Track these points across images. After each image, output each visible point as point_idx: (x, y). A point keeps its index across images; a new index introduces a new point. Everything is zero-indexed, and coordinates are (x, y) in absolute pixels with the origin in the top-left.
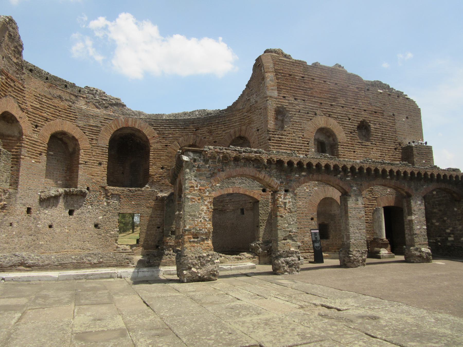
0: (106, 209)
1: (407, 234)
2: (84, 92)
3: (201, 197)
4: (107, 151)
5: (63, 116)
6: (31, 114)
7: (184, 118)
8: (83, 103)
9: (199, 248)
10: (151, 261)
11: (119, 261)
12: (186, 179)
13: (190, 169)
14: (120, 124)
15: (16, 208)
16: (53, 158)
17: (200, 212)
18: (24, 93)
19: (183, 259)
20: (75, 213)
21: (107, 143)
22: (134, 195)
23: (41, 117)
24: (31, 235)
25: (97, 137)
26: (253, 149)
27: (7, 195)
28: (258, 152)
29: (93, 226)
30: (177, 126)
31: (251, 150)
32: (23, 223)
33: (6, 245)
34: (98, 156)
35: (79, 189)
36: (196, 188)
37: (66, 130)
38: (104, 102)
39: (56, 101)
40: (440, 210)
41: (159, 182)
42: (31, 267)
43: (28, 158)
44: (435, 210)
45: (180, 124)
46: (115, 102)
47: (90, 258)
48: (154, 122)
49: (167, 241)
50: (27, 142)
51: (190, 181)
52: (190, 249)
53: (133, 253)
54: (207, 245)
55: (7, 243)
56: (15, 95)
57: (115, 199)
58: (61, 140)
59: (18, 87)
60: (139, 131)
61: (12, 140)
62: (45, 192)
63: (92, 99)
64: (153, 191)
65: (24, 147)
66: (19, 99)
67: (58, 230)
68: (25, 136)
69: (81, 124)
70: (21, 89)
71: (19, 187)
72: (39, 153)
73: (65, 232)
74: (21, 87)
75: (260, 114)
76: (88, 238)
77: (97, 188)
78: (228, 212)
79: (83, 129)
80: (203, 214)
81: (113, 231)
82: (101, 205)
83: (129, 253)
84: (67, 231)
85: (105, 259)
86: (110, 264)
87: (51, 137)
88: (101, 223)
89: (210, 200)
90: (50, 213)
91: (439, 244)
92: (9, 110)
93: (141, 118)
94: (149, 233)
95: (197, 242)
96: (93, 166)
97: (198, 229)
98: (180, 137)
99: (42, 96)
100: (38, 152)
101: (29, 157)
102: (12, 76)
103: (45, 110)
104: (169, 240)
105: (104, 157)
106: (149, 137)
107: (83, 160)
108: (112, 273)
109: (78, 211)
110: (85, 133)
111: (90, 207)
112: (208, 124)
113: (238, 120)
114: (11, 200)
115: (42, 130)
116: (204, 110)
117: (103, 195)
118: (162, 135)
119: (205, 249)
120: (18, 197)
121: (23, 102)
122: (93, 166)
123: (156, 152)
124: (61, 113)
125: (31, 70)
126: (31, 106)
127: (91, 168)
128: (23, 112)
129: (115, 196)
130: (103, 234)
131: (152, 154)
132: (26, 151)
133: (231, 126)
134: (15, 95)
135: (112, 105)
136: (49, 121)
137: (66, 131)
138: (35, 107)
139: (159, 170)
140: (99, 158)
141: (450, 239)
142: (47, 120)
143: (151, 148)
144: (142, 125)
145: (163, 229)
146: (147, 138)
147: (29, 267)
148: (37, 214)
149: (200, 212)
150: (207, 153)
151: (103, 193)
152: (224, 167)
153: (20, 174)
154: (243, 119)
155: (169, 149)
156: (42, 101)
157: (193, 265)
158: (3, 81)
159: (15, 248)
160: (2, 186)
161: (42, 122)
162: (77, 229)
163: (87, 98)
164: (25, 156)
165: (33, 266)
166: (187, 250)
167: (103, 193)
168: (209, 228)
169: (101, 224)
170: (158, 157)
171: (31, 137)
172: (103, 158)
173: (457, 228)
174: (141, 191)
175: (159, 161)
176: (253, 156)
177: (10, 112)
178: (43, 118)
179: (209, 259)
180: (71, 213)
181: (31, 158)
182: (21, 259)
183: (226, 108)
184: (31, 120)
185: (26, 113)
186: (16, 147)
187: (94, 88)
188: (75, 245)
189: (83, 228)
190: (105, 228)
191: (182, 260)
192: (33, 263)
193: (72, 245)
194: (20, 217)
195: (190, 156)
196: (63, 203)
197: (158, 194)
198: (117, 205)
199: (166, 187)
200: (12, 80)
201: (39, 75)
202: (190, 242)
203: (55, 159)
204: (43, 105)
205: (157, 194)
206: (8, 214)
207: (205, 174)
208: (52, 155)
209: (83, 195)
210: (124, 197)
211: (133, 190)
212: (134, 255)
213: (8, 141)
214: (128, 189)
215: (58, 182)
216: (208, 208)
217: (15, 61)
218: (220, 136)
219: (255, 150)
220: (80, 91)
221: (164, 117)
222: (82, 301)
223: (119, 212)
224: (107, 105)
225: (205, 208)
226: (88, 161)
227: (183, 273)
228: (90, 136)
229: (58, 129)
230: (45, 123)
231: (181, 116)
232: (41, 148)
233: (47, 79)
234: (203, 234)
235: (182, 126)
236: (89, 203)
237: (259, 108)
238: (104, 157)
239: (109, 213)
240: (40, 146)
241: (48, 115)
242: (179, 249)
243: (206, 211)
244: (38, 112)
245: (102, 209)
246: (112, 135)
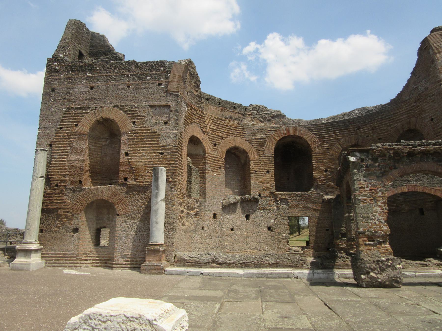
0: (276, 213)
2: (249, 110)
3: (373, 198)
4: (273, 160)
5: (234, 133)
6: (211, 135)
7: (344, 119)
8: (249, 120)
9: (376, 251)
10: (324, 264)
11: (294, 262)
12: (355, 180)
13: (358, 170)
14: (282, 134)
15: (205, 215)
16: (229, 170)
17: (374, 213)
18: (204, 119)
19: (360, 262)
20: (250, 218)
21: (272, 152)
22: (301, 199)
23: (218, 137)
24: (218, 237)
25: (263, 148)
26: (430, 141)
27: (198, 204)
28: (438, 144)
29: (267, 228)
30: (337, 128)
31: (428, 142)
32: (212, 227)
33: (200, 245)
34: (266, 165)
35: (252, 196)
36: (366, 189)
37: (237, 145)
38: (267, 116)
39: (228, 121)
41: (324, 185)
42: (221, 264)
43: (211, 172)
45: (340, 126)
46: (276, 114)
47: (268, 258)
48: (313, 127)
49: (338, 243)
50: (210, 158)
51: (359, 182)
52: (367, 253)
53: (304, 255)
54: (385, 248)
55: (201, 244)
56: (198, 122)
57: (284, 204)
58: (234, 154)
59: (200, 115)
60: (300, 138)
61: (198, 158)
62: (225, 199)
63: (256, 115)
64: (318, 194)
65: (208, 163)
66: (201, 124)
67: (238, 233)
68: (208, 154)
69: (249, 138)
70: (202, 116)
71: (207, 196)
72: (219, 167)
73: (244, 234)
74: (202, 114)
75: (433, 101)
76: (264, 239)
77: (267, 194)
78: (403, 212)
79: (251, 142)
80: (377, 216)
81: (284, 234)
82: (272, 210)
84: (245, 233)
85: (281, 260)
86: (286, 264)
87: (226, 153)
88: (273, 226)
89: (384, 201)
90: (231, 218)
92: (194, 134)
93: (301, 126)
94: (318, 235)
95: (373, 246)
96: (262, 175)
97: (373, 231)
98: (341, 139)
99: (217, 119)
100: (218, 166)
101: (211, 171)
102: (195, 106)
103: (220, 131)
104: (339, 242)
105: (270, 165)
106: (310, 143)
107: (253, 169)
108: (289, 273)
109: (253, 215)
110: (253, 145)
111: (262, 211)
112: (369, 122)
113: (405, 112)
114: (202, 208)
115: (219, 147)
116: (364, 108)
117: (273, 200)
118: (322, 139)
119: (383, 253)
120: (207, 205)
121: (204, 126)
122: (262, 175)
123: (318, 155)
124: (232, 131)
125: (207, 99)
126: (210, 128)
127: (261, 177)
128: (205, 134)
129: (284, 200)
130: (276, 237)
131: (315, 158)
132: (209, 166)
133: (397, 120)
134: (198, 122)
135: (273, 117)
136: (224, 139)
137: (238, 146)
138: (213, 129)
139: (323, 173)
140: (267, 167)
142: (222, 138)
143: (313, 153)
144: (302, 132)
145: (332, 232)
146: (308, 143)
147: (220, 264)
148: (221, 219)
149: (374, 213)
150: (375, 151)
151: (272, 199)
152: (397, 165)
153: (207, 186)
154: (412, 110)
155: (331, 152)
156: (217, 123)
157: (371, 269)
158: (189, 111)
159: (207, 248)
160: (195, 196)
161: (219, 141)
162: (253, 232)
163: (252, 115)
164: (209, 171)
165: (223, 264)
166: (363, 254)
167: (272, 199)
168: (386, 230)
169: (273, 227)
170: (320, 161)
171: (212, 154)
172: (270, 166)
174: (307, 194)
175: (321, 165)
176: (432, 149)
177: (196, 135)
178: (219, 137)
179: (389, 264)
180: (247, 217)
181: (213, 171)
182: (213, 257)
183: (389, 101)
184: (211, 140)
185: (207, 135)
186: (202, 164)
187: (257, 105)
188: (253, 246)
189: (258, 231)
190: (277, 231)
191: (359, 264)
192: (222, 261)
193: (250, 246)
194: (209, 222)
195: (356, 156)
196: (241, 209)
197: (324, 196)
198: (286, 209)
199: (331, 190)
200: (195, 110)
201: (213, 102)
202: (366, 245)
203: (231, 171)
204: (219, 126)
205: (323, 197)
206: (200, 220)
207: (375, 173)
208: (229, 168)
209: (256, 201)
210: (292, 201)
211: (299, 194)
212: (305, 256)
213: (196, 159)
214: (295, 194)
215: (235, 191)
216: (383, 209)
217: (196, 93)
218: (384, 133)
219: (433, 142)
220: (246, 110)
221: (323, 121)
222: (268, 298)
223: (288, 215)
224: (269, 118)
225: (379, 209)
226: (258, 170)
227: (361, 277)
228: (257, 148)
229: (232, 145)
230: (221, 141)
231: (340, 118)
232: (220, 162)
233: (220, 104)
234: (379, 237)
235: (342, 128)
236: (261, 208)
237: (430, 95)
238: (270, 165)
239: (279, 216)
240: (219, 161)
241: (223, 134)
242: (353, 252)
243: (380, 212)
244: (215, 133)
245: (273, 213)
246: (276, 145)
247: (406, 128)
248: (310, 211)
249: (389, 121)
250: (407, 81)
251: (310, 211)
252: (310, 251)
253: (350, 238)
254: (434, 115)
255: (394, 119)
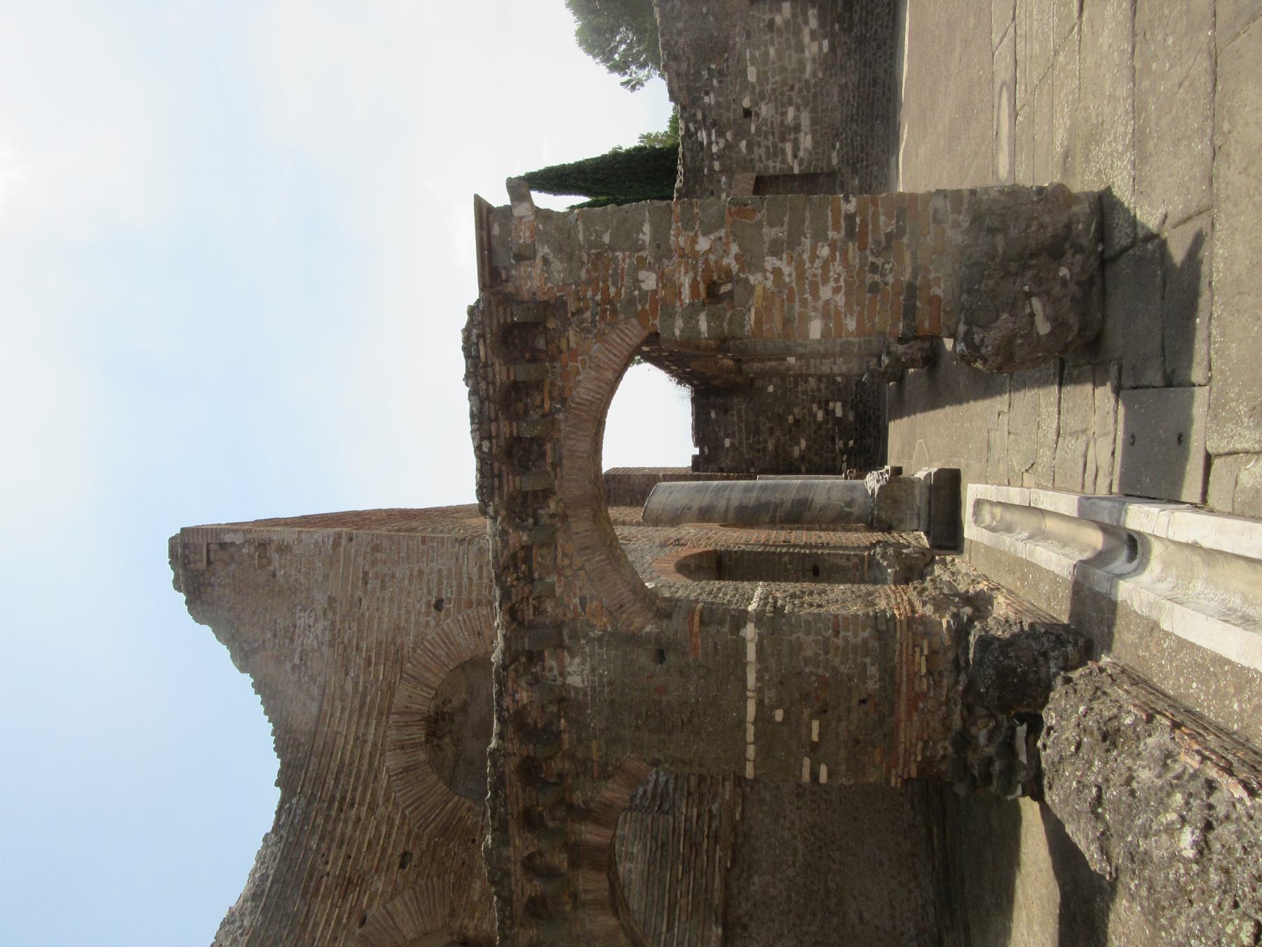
1: (831, 369)
40: (771, 431)
44: (770, 447)
91: (851, 443)
112: (304, 895)
113: (358, 724)
133: (370, 764)
141: (839, 413)
173: (812, 390)
183: (278, 792)
218: (388, 835)
247: (419, 734)
249: (352, 805)
250: (256, 693)
253: (875, 628)
254: (429, 593)
255: (357, 779)
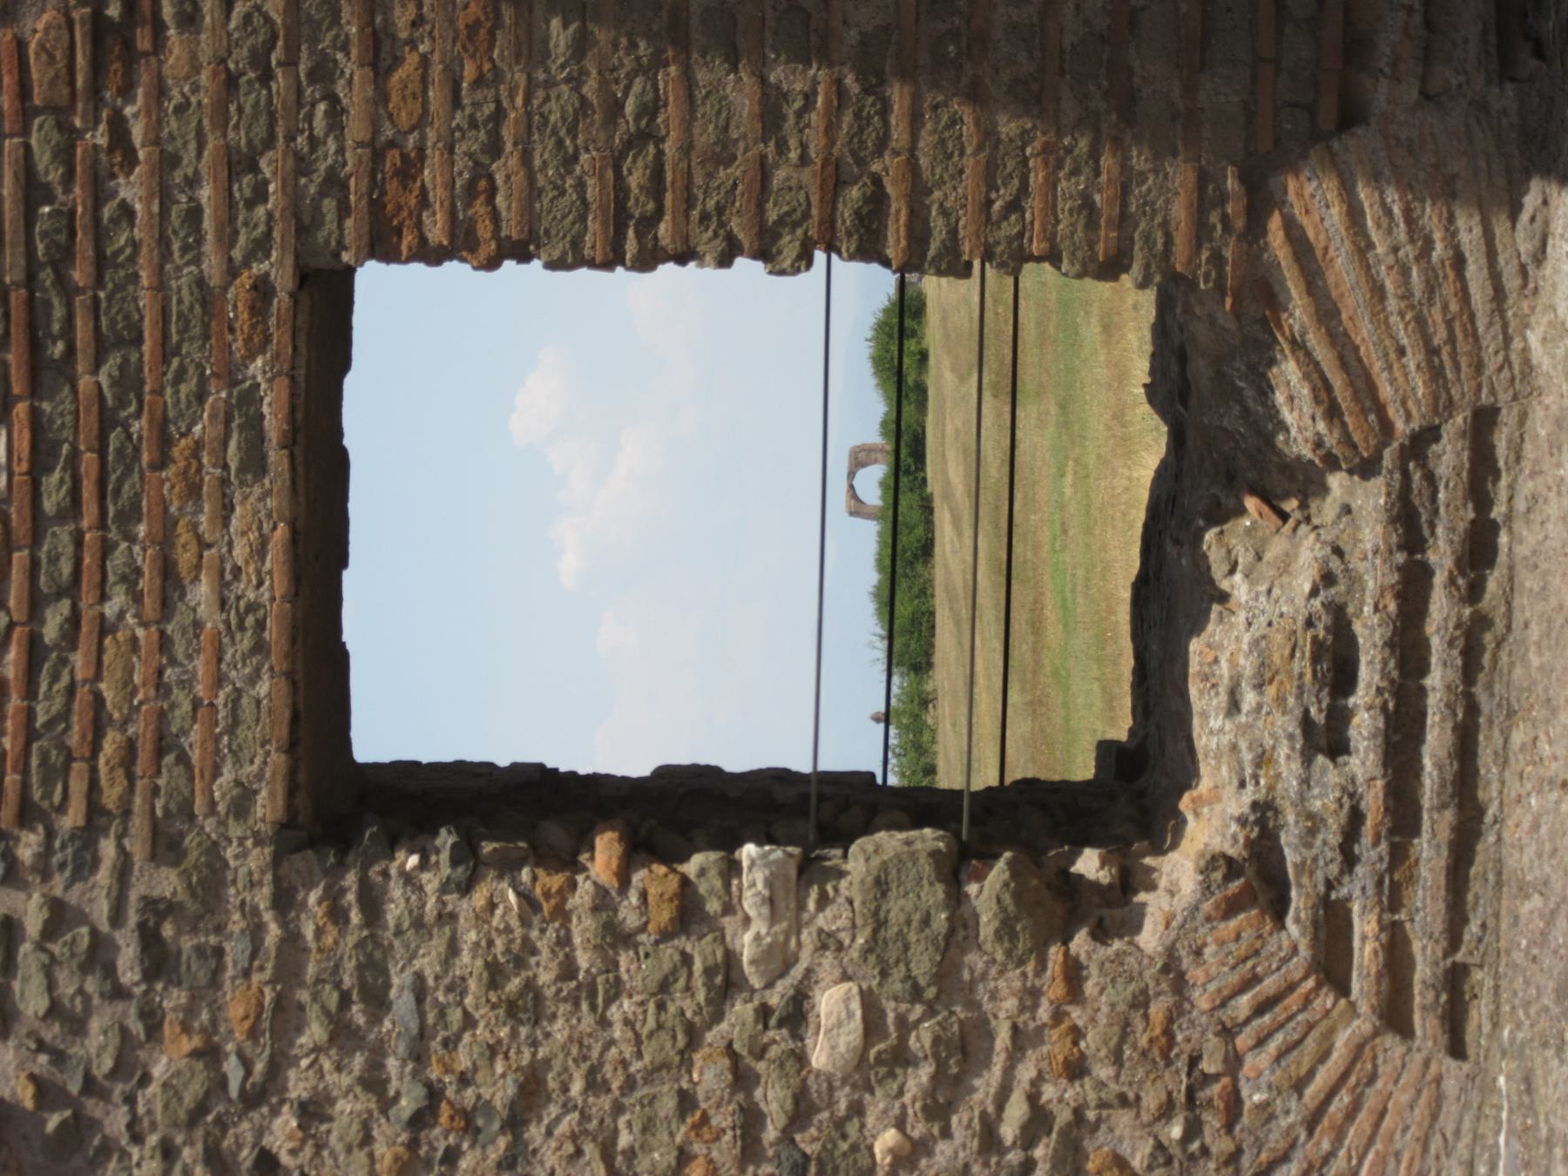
53: (1449, 456)
81: (797, 1015)
83: (1441, 556)
198: (59, 917)
212: (1483, 421)
248: (131, 189)
251: (131, 189)
252: (1341, 268)
